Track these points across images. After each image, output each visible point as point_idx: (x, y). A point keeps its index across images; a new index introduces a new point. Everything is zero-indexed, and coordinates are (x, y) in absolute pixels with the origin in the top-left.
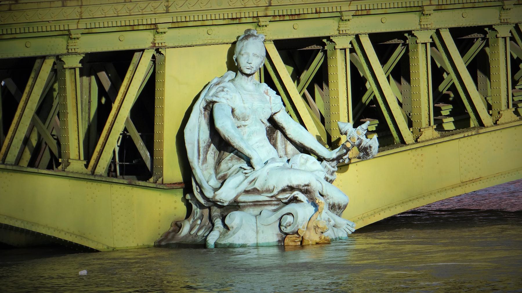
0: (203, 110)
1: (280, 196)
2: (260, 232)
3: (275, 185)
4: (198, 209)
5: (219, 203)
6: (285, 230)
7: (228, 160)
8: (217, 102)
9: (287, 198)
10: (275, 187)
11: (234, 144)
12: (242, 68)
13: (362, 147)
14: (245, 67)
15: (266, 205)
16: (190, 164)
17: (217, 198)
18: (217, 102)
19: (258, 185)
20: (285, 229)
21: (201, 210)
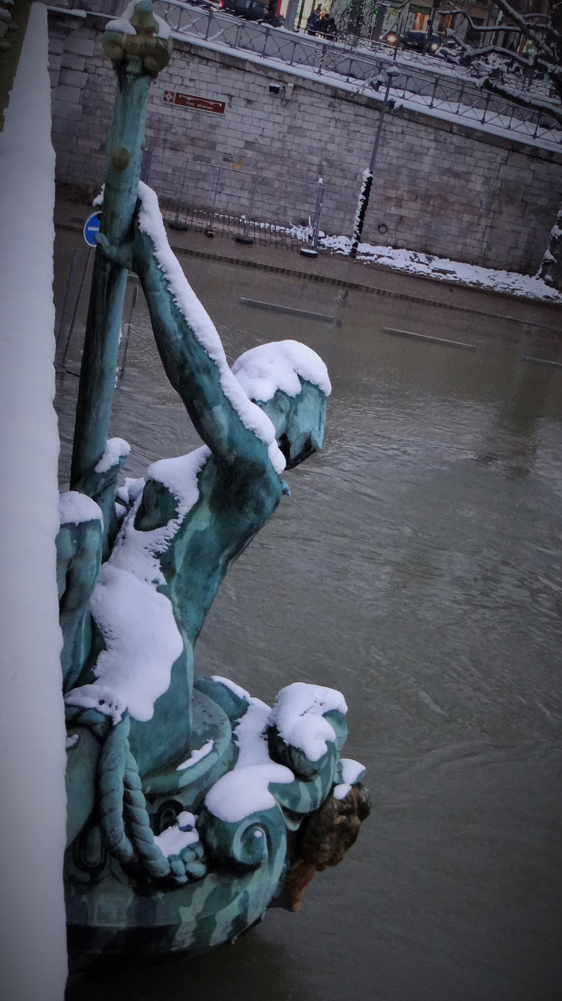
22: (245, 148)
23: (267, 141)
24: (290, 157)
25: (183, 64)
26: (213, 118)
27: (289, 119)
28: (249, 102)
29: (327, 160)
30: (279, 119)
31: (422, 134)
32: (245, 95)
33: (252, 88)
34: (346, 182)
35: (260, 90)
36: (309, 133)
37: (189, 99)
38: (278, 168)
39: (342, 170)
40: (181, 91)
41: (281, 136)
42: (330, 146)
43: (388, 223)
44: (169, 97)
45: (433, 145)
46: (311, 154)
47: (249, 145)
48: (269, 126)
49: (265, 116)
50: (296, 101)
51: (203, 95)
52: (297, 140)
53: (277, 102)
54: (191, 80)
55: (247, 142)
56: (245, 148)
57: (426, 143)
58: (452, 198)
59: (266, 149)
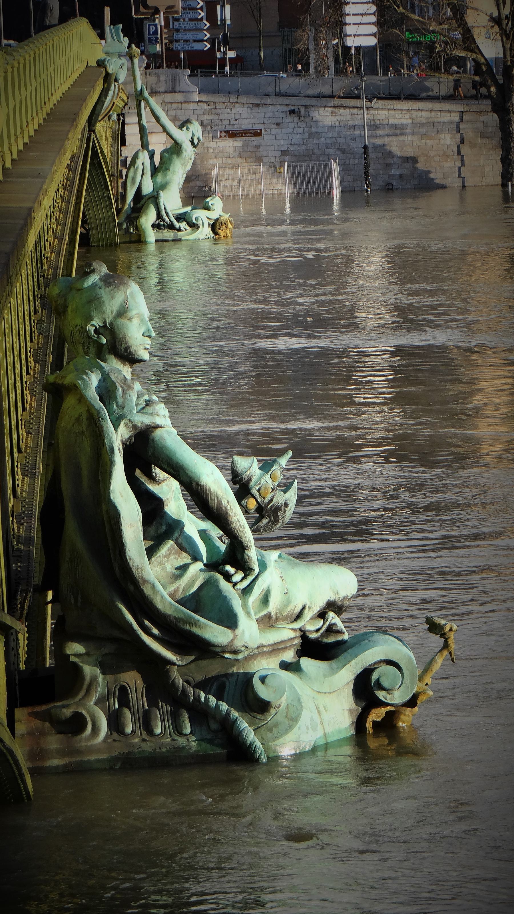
0: (121, 447)
1: (309, 627)
2: (322, 709)
3: (308, 604)
4: (100, 677)
5: (227, 655)
6: (391, 699)
7: (165, 557)
8: (161, 427)
9: (318, 630)
10: (307, 608)
11: (233, 520)
12: (133, 349)
13: (273, 505)
14: (142, 347)
15: (285, 648)
16: (135, 573)
17: (238, 644)
18: (161, 427)
19: (272, 608)
20: (388, 697)
21: (110, 677)
22: (282, 155)
23: (296, 147)
24: (314, 154)
25: (228, 110)
27: (307, 129)
28: (278, 124)
29: (339, 149)
32: (274, 121)
33: (277, 114)
34: (356, 161)
35: (284, 115)
36: (323, 135)
37: (237, 132)
38: (308, 164)
39: (352, 154)
40: (230, 128)
41: (305, 141)
42: (340, 140)
43: (392, 182)
44: (223, 134)
46: (328, 148)
48: (295, 137)
49: (290, 131)
50: (309, 116)
51: (246, 127)
52: (316, 142)
53: (296, 119)
54: (236, 120)
55: (282, 151)
56: (282, 155)
58: (432, 154)
59: (296, 153)
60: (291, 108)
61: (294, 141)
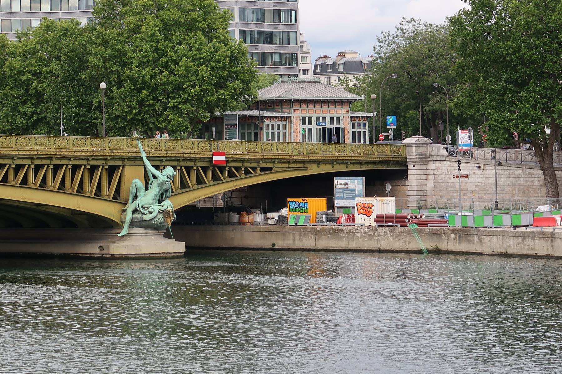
26: (465, 180)
28: (474, 173)
30: (482, 176)
31: (519, 171)
45: (523, 173)
47: (476, 186)
48: (480, 179)
57: (521, 173)
58: (530, 190)
59: (480, 187)
60: (478, 165)
61: (480, 181)
